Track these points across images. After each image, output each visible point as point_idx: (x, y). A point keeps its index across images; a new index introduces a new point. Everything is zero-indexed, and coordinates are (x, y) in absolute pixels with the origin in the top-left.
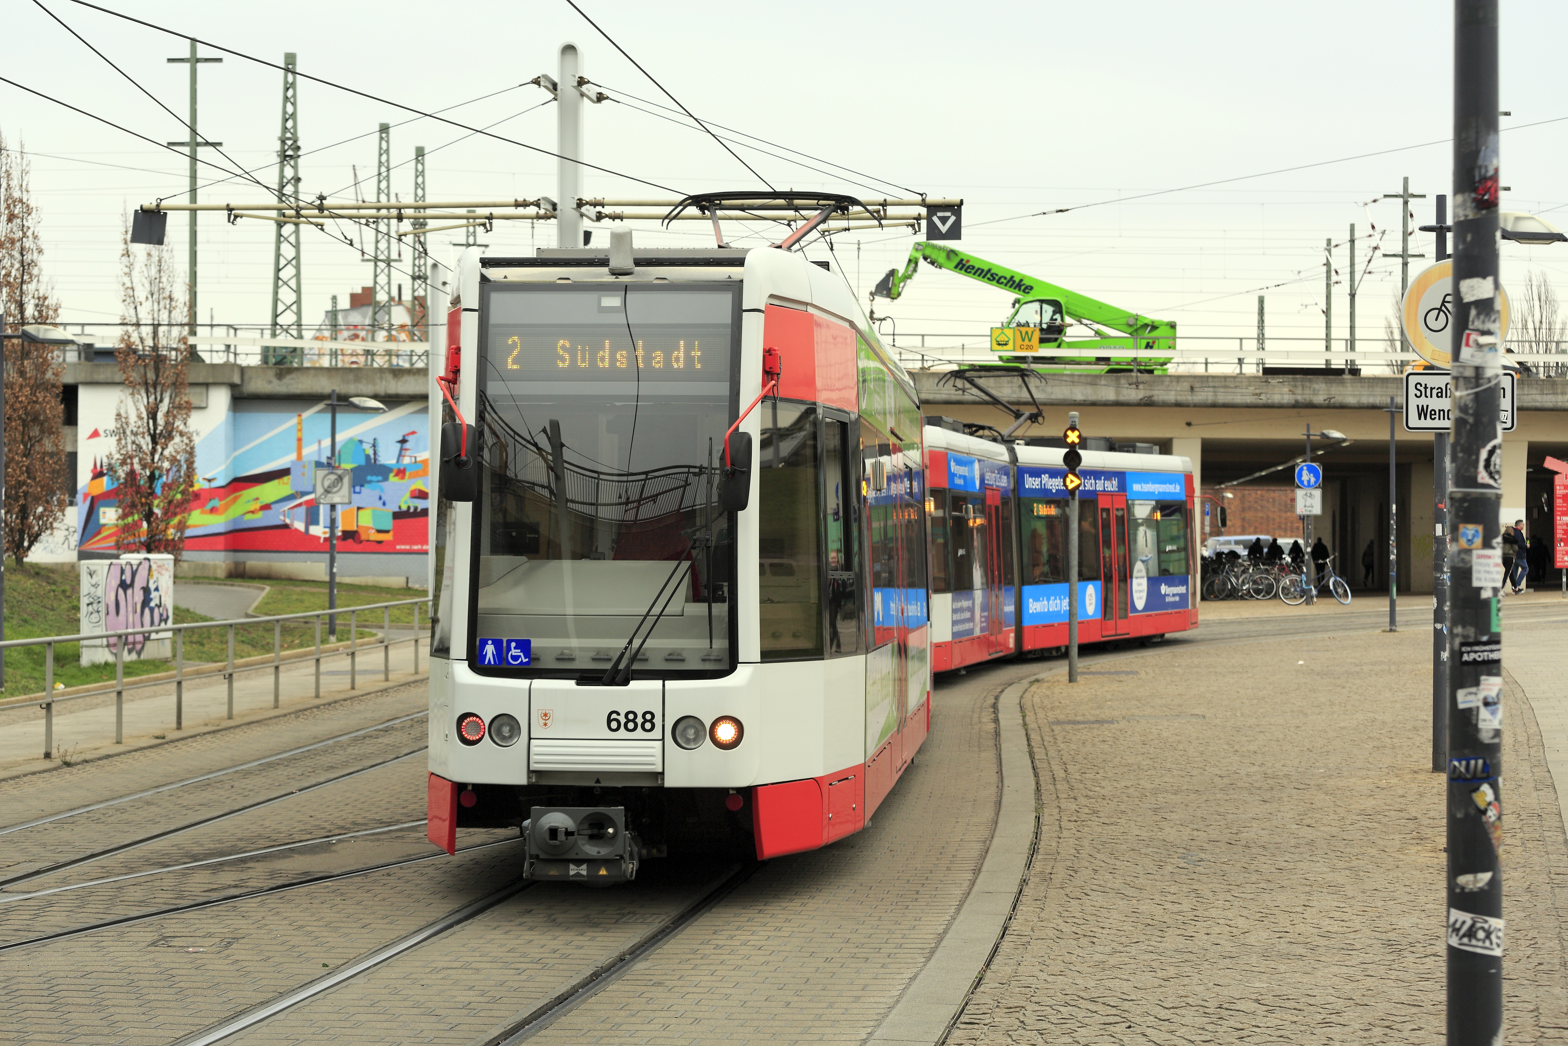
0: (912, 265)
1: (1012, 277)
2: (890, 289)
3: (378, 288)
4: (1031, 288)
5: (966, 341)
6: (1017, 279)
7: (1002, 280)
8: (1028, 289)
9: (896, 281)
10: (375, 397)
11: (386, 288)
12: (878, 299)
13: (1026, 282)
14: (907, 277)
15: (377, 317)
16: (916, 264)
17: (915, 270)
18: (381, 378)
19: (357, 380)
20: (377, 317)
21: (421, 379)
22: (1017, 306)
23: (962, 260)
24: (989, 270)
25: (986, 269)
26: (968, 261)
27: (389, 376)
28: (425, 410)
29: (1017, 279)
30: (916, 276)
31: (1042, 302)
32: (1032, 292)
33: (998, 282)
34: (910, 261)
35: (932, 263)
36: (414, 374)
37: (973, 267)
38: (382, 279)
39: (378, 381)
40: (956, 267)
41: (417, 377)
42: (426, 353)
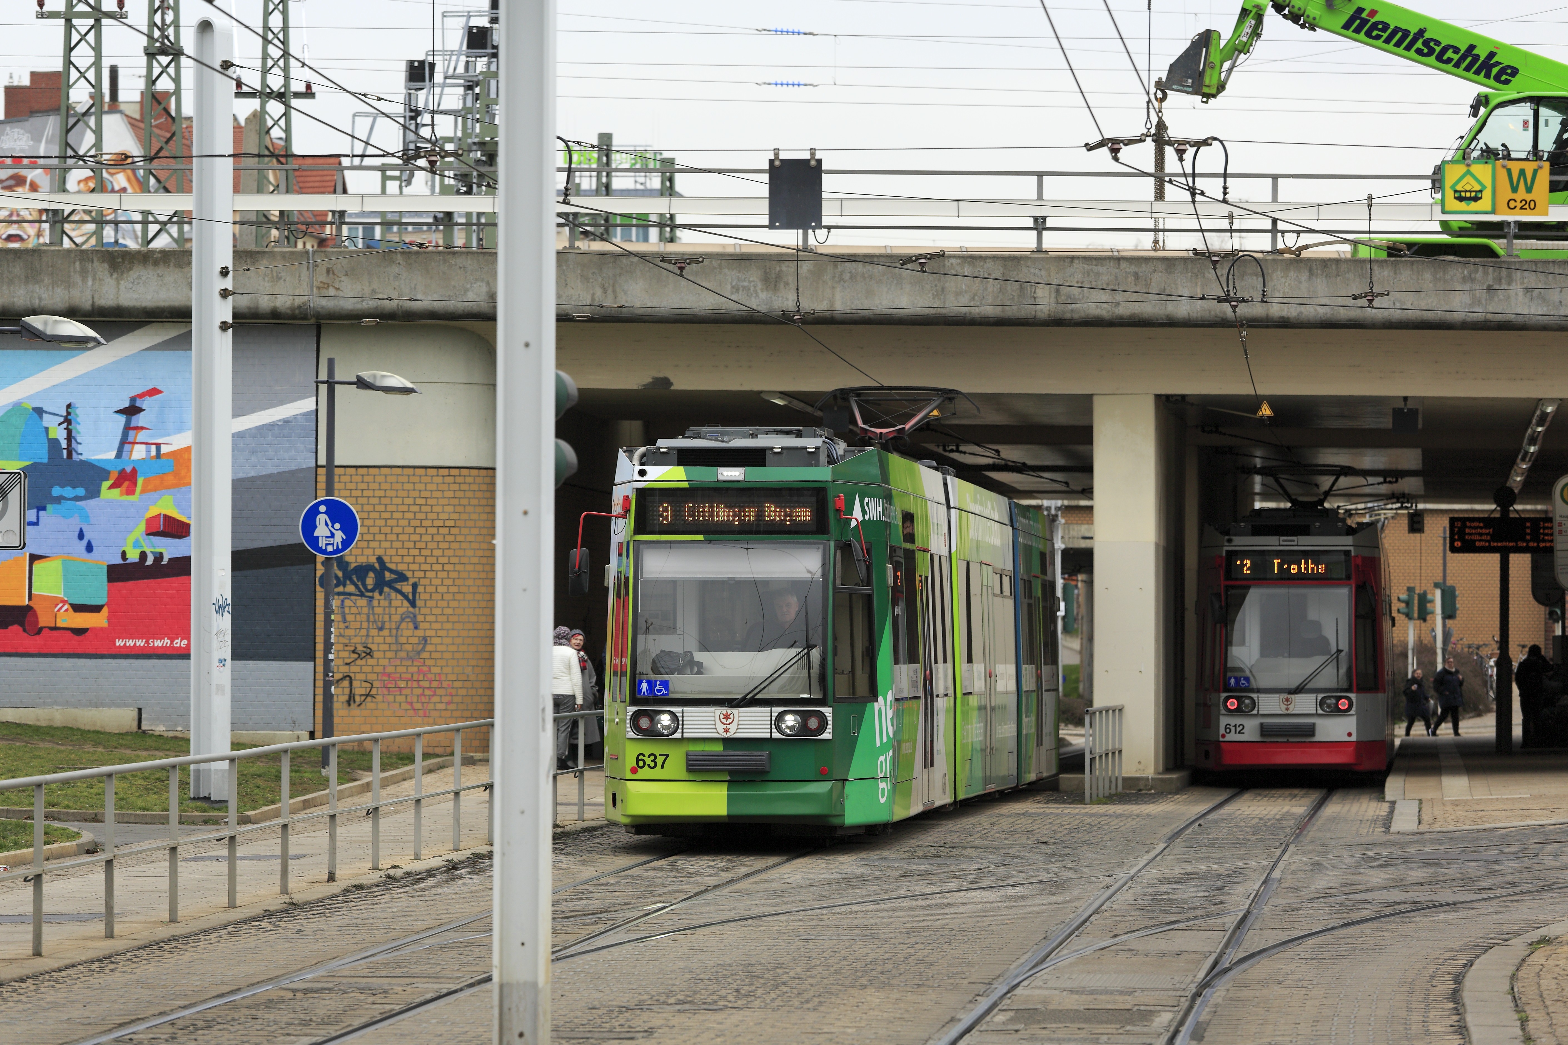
0: (1250, 22)
1: (1472, 47)
2: (1201, 74)
3: (74, 74)
4: (1515, 72)
5: (1376, 188)
6: (1482, 53)
7: (1449, 54)
8: (1507, 74)
9: (1215, 57)
10: (72, 313)
11: (91, 75)
12: (1173, 96)
13: (1501, 58)
14: (1240, 48)
15: (72, 138)
16: (1259, 18)
17: (1256, 33)
18: (84, 273)
19: (32, 276)
20: (72, 138)
21: (171, 275)
22: (1482, 110)
23: (1360, 10)
24: (1421, 32)
25: (1414, 30)
26: (1373, 13)
27: (102, 269)
28: (184, 341)
29: (1482, 53)
30: (1259, 46)
31: (1538, 101)
32: (1515, 81)
33: (1439, 58)
34: (1244, 12)
35: (1295, 18)
36: (156, 263)
37: (1386, 26)
38: (83, 56)
39: (77, 279)
40: (1346, 26)
41: (160, 270)
42: (181, 218)
